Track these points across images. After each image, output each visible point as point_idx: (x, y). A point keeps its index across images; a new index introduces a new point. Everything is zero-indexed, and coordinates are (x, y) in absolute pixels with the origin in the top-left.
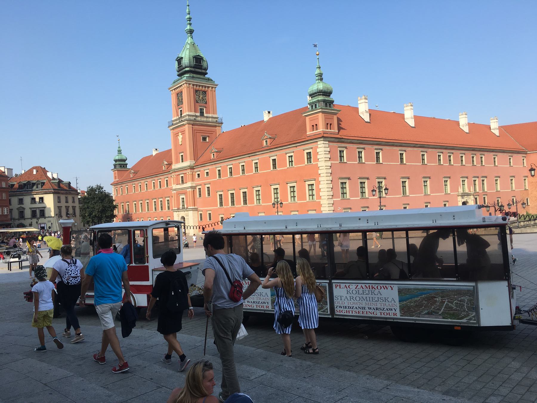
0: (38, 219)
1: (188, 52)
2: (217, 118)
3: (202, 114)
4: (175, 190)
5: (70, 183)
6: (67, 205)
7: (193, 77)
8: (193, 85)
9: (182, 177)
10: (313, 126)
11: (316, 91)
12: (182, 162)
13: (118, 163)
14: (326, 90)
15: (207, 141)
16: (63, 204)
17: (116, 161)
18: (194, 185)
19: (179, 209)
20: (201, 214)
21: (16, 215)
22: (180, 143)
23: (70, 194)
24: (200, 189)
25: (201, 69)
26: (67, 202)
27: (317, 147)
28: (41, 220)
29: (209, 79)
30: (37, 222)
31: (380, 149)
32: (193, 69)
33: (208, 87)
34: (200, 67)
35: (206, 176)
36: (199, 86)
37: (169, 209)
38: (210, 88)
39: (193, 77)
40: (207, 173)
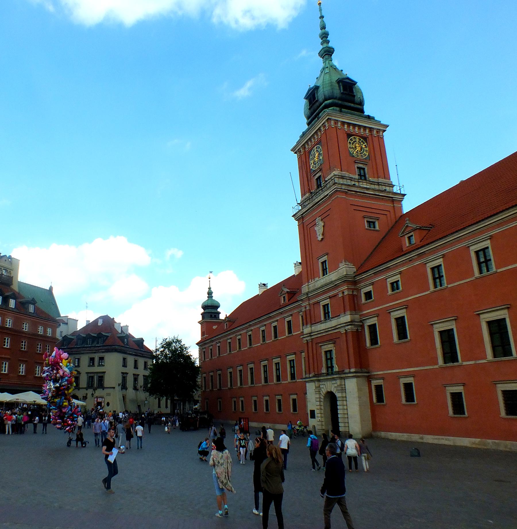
1: (327, 76)
3: (363, 177)
4: (310, 334)
9: (326, 306)
12: (324, 275)
13: (207, 311)
15: (377, 228)
18: (357, 317)
19: (321, 375)
20: (379, 388)
22: (320, 238)
24: (373, 328)
32: (340, 102)
35: (390, 292)
37: (293, 377)
39: (341, 111)
40: (395, 286)
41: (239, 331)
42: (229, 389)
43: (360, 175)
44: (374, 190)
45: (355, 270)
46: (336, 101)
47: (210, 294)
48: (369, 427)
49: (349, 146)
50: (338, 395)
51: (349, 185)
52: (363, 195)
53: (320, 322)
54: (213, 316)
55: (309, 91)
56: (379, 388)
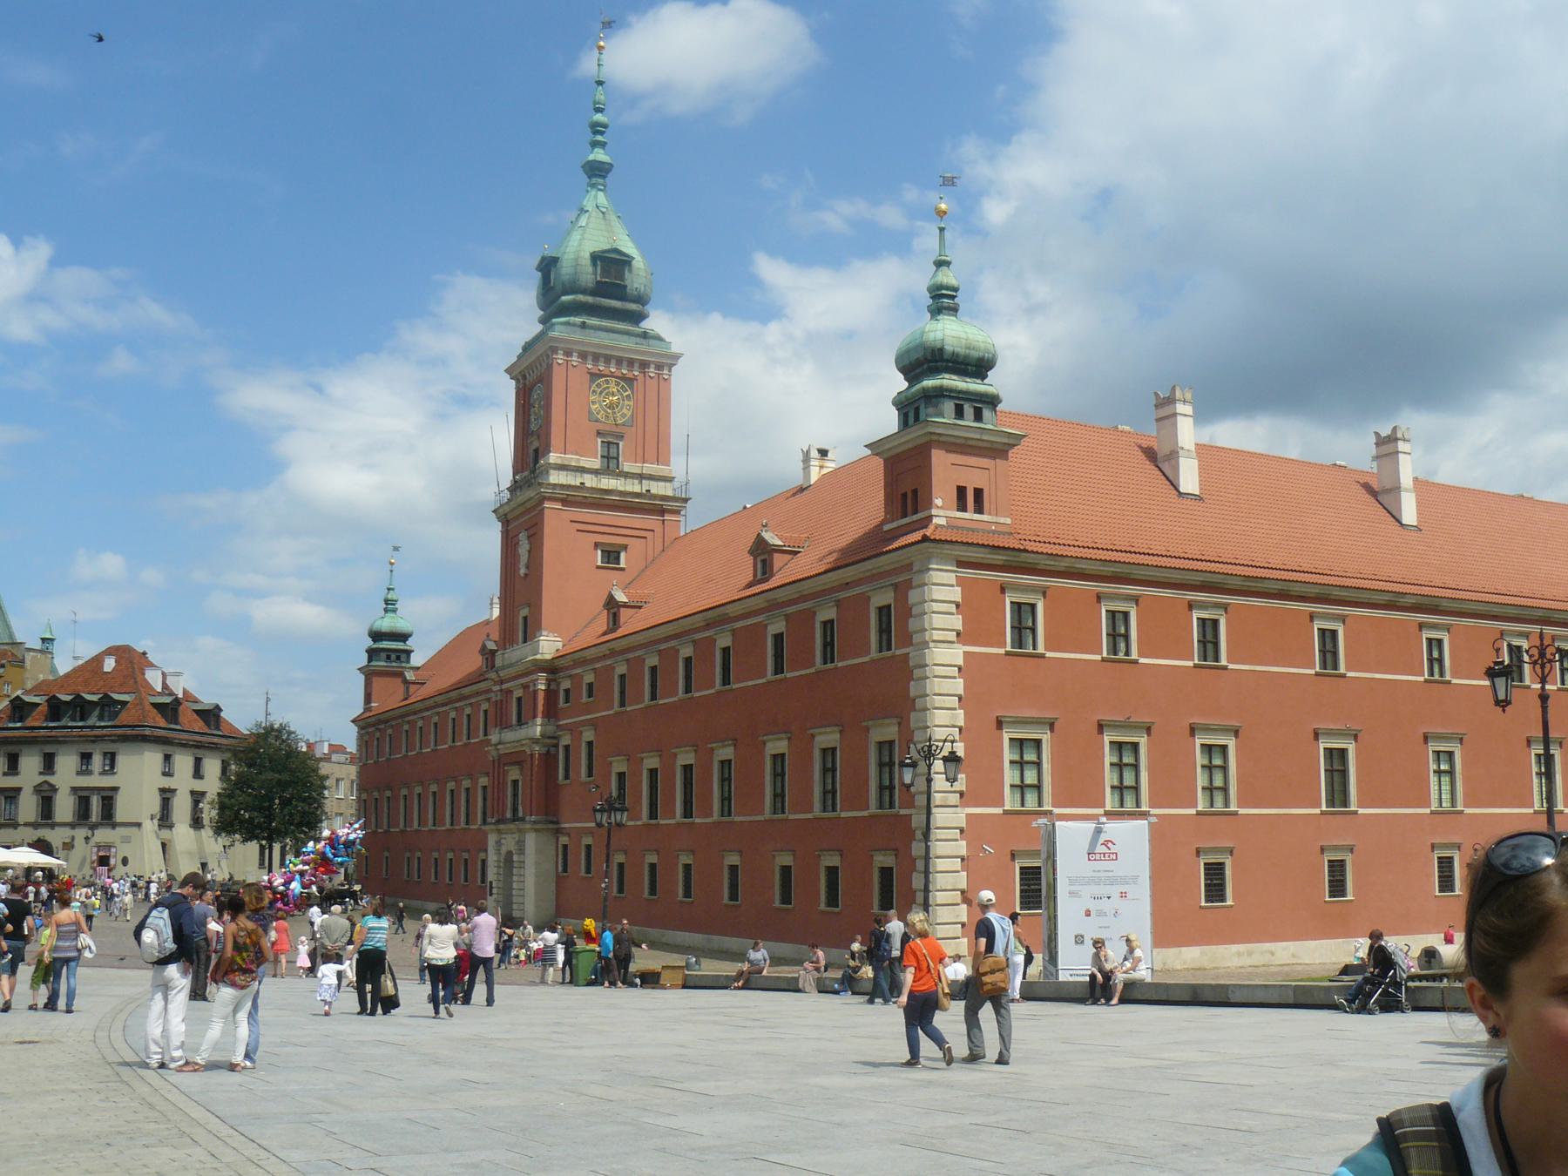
0: (93, 827)
2: (670, 479)
5: (218, 708)
6: (198, 786)
7: (583, 325)
8: (583, 356)
10: (904, 495)
11: (920, 355)
14: (962, 351)
16: (183, 780)
17: (376, 636)
18: (551, 729)
20: (565, 847)
21: (28, 807)
22: (522, 571)
23: (213, 748)
25: (623, 298)
26: (198, 774)
27: (908, 585)
28: (103, 835)
29: (645, 335)
30: (87, 839)
31: (1217, 606)
32: (590, 299)
33: (644, 365)
34: (619, 291)
35: (585, 699)
36: (608, 359)
38: (652, 371)
39: (583, 325)
41: (420, 711)
42: (402, 831)
43: (606, 457)
44: (622, 493)
45: (560, 645)
46: (581, 297)
47: (390, 605)
48: (552, 910)
49: (592, 398)
50: (515, 858)
51: (569, 487)
52: (600, 500)
53: (508, 727)
54: (393, 657)
55: (543, 259)
56: (565, 847)
